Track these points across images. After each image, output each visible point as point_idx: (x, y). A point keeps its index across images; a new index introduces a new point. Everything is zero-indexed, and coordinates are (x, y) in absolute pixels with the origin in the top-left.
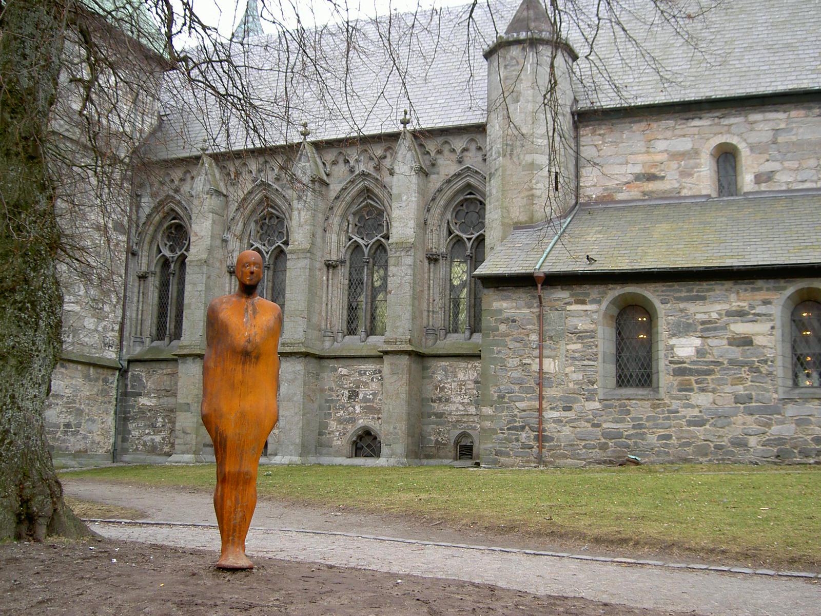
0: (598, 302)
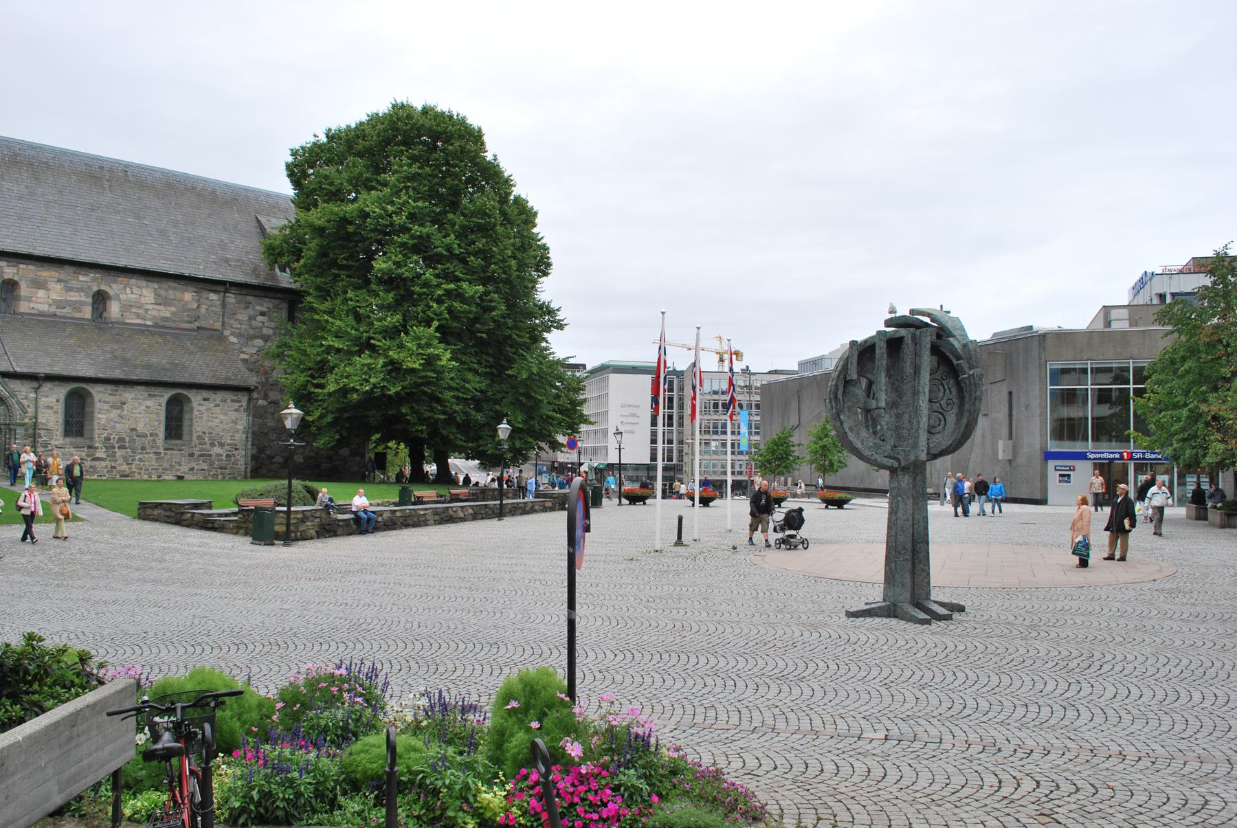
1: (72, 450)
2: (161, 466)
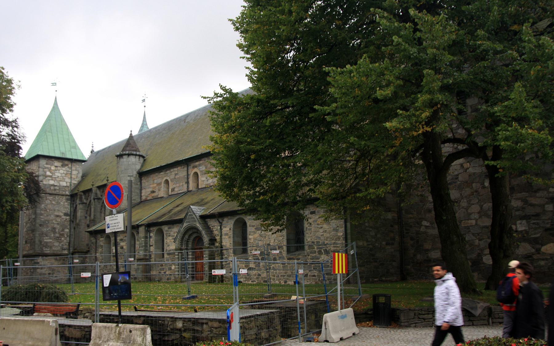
0: (103, 237)
2: (286, 273)
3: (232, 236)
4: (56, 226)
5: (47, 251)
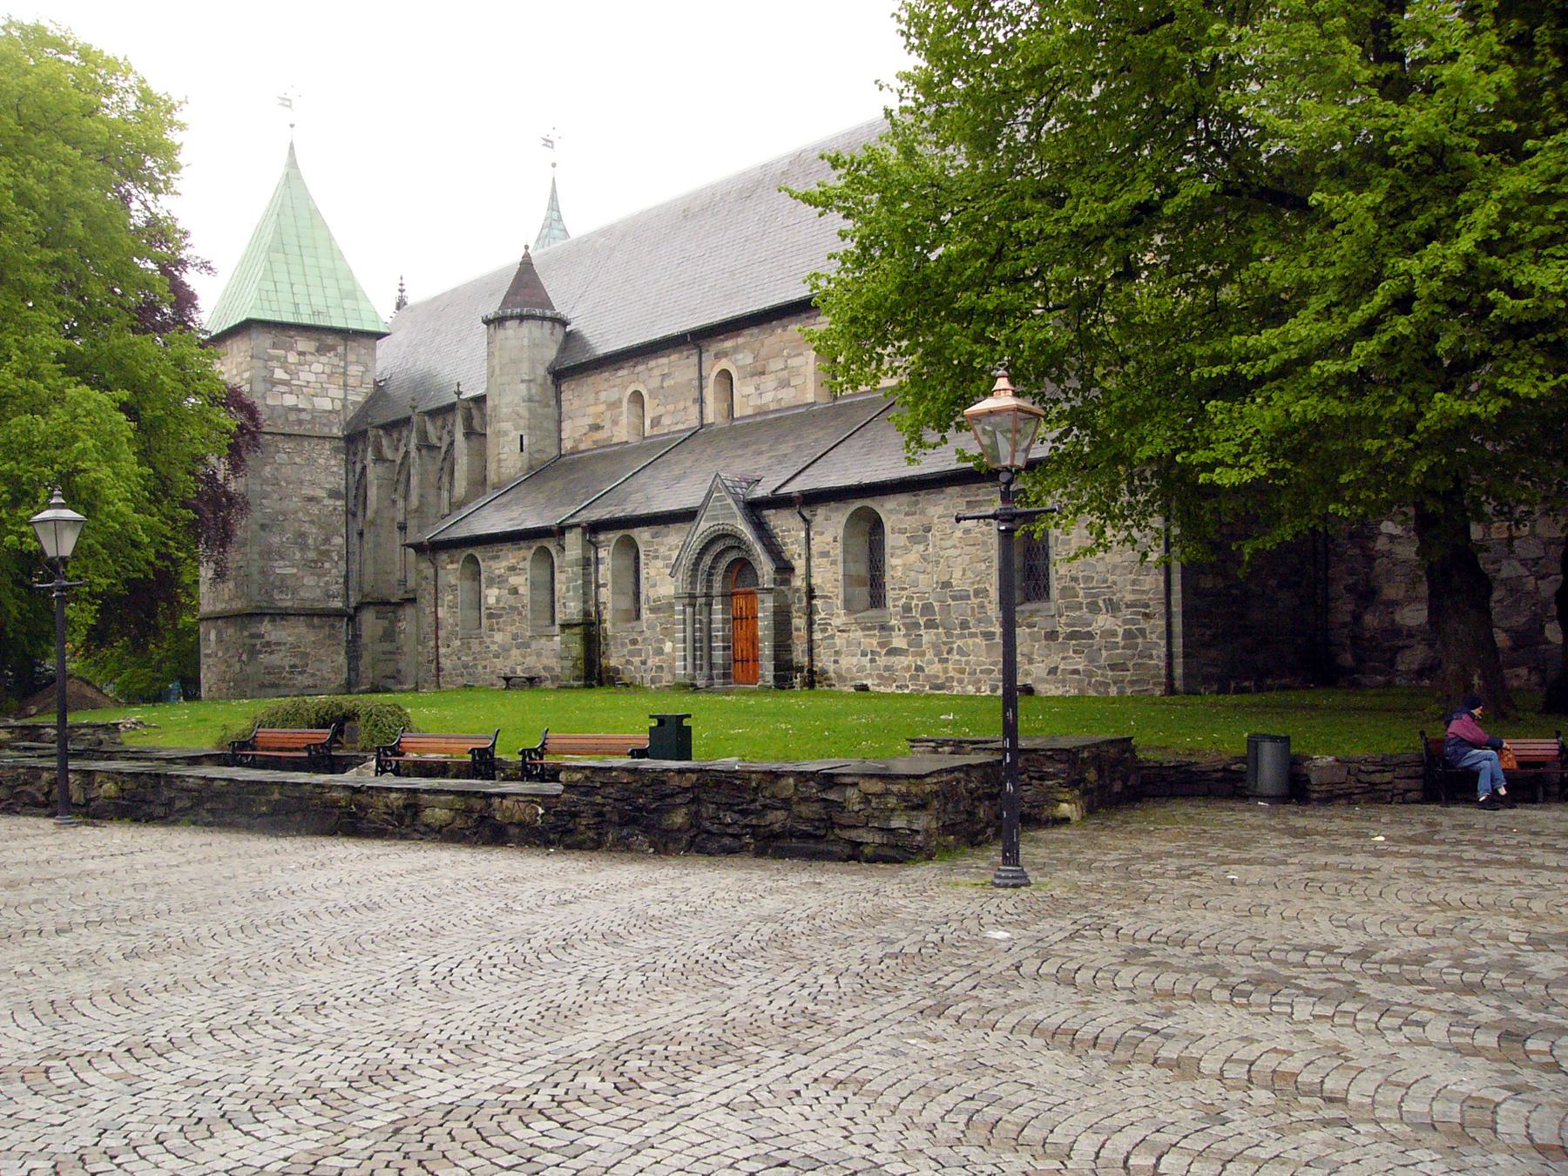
0: (457, 562)
1: (860, 633)
3: (840, 558)
4: (306, 528)
5: (285, 601)
